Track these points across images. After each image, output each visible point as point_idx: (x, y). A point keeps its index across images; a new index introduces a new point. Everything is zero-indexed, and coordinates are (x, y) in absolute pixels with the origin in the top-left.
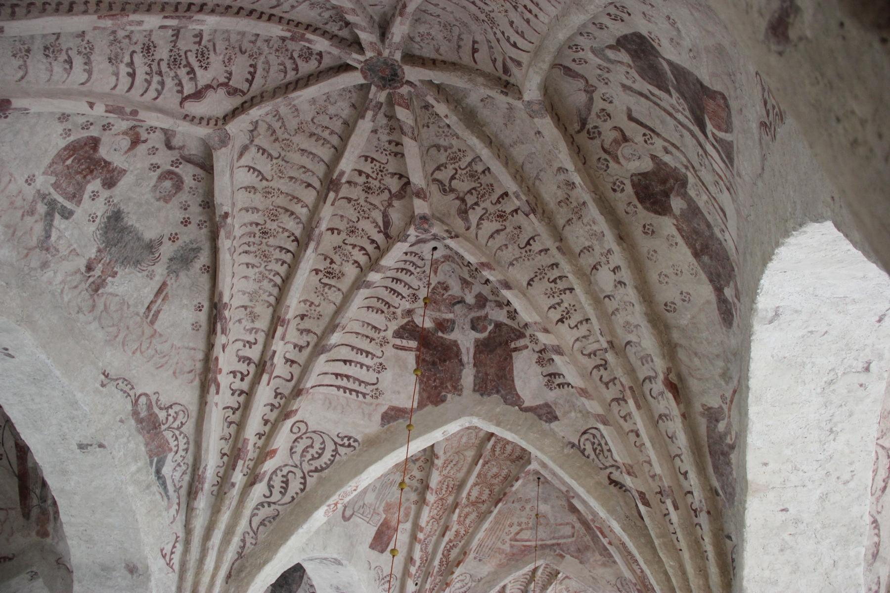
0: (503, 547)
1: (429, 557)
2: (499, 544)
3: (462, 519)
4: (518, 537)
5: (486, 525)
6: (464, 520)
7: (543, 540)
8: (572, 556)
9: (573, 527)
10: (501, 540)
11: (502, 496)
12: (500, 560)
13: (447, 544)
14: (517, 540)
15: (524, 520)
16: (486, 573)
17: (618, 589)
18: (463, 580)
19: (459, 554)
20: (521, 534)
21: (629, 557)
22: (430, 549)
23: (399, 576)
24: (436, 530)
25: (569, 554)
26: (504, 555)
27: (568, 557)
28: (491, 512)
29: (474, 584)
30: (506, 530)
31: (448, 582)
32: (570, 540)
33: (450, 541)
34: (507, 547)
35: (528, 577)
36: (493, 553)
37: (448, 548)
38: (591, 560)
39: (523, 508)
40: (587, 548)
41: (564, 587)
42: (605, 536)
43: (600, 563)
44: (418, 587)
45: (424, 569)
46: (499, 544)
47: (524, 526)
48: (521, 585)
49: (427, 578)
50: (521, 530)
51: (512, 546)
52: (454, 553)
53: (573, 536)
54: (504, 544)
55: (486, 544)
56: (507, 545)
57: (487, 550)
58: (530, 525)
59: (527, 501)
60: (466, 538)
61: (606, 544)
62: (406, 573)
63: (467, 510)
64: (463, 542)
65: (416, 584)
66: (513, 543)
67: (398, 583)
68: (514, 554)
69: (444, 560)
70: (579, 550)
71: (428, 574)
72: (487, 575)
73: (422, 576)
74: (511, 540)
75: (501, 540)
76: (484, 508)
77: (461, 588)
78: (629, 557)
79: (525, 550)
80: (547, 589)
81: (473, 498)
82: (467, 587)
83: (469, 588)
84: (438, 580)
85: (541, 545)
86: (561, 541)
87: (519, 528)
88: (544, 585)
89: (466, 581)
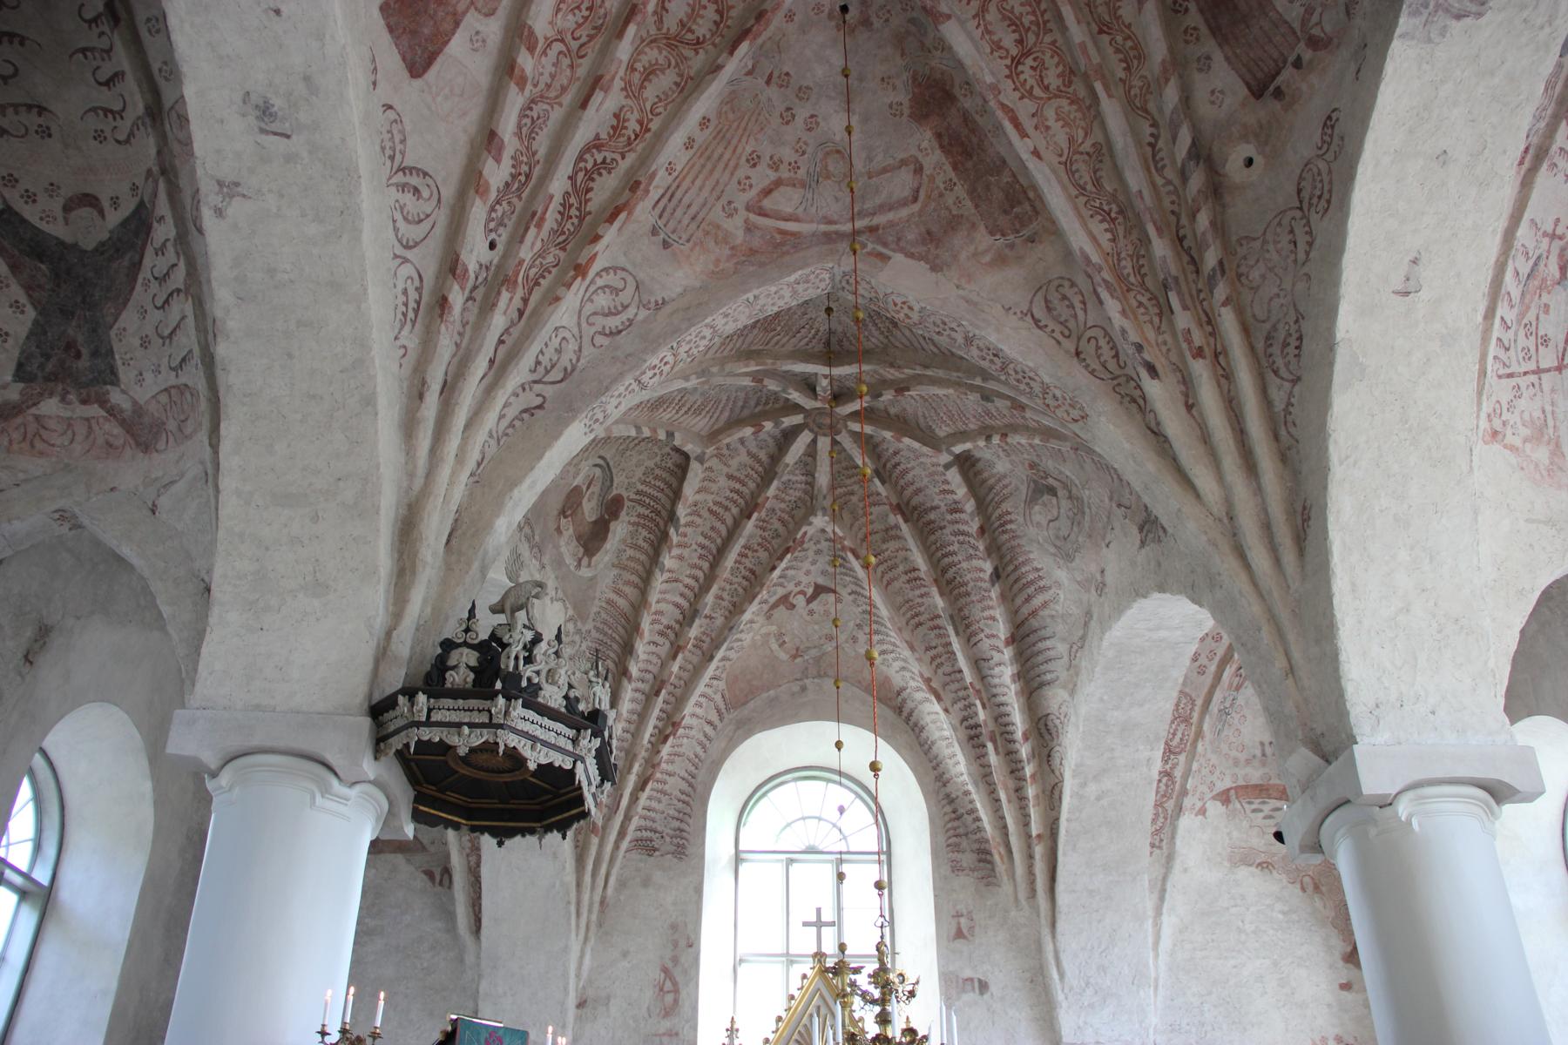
0: (728, 224)
1: (537, 171)
2: (717, 214)
3: (636, 78)
4: (767, 203)
5: (706, 103)
6: (642, 87)
7: (830, 222)
8: (911, 256)
9: (919, 170)
10: (723, 201)
11: (752, 21)
12: (718, 261)
13: (587, 149)
14: (763, 213)
15: (787, 154)
16: (679, 290)
17: (1036, 321)
18: (616, 291)
19: (617, 193)
20: (775, 194)
21: (1082, 199)
22: (542, 145)
23: (448, 192)
24: (564, 89)
25: (902, 250)
26: (727, 252)
27: (898, 258)
28: (719, 68)
29: (643, 314)
30: (740, 174)
31: (582, 260)
32: (904, 213)
33: (596, 144)
34: (735, 226)
35: (700, 574)
36: (700, 234)
37: (589, 166)
38: (963, 256)
39: (788, 117)
40: (954, 223)
41: (774, 628)
42: (1023, 134)
43: (987, 258)
44: (495, 256)
45: (519, 205)
46: (717, 214)
47: (785, 173)
48: (682, 595)
49: (527, 229)
50: (778, 183)
51: (749, 228)
52: (604, 188)
53: (915, 199)
54: (730, 216)
55: (686, 201)
56: (738, 220)
57: (686, 221)
58: (802, 173)
59: (803, 93)
60: (640, 147)
61: (1025, 156)
62: (472, 180)
63: (652, 55)
64: (631, 158)
65: (492, 246)
66: (753, 217)
67: (442, 217)
68: (753, 252)
69: (572, 200)
70: (929, 237)
71: (530, 218)
72: (681, 295)
73: (510, 224)
74: (748, 208)
75: (723, 201)
76: (697, 61)
77: (610, 314)
78: (1082, 199)
79: (782, 244)
80: (743, 612)
81: (671, 23)
82: (624, 317)
83: (631, 321)
84: (550, 259)
85: (826, 235)
86: (880, 220)
87: (773, 176)
88: (734, 605)
89: (625, 297)
